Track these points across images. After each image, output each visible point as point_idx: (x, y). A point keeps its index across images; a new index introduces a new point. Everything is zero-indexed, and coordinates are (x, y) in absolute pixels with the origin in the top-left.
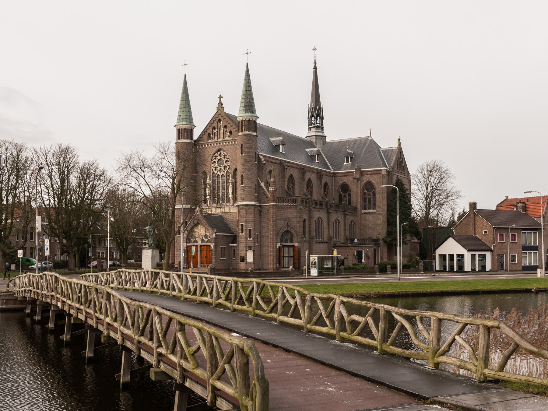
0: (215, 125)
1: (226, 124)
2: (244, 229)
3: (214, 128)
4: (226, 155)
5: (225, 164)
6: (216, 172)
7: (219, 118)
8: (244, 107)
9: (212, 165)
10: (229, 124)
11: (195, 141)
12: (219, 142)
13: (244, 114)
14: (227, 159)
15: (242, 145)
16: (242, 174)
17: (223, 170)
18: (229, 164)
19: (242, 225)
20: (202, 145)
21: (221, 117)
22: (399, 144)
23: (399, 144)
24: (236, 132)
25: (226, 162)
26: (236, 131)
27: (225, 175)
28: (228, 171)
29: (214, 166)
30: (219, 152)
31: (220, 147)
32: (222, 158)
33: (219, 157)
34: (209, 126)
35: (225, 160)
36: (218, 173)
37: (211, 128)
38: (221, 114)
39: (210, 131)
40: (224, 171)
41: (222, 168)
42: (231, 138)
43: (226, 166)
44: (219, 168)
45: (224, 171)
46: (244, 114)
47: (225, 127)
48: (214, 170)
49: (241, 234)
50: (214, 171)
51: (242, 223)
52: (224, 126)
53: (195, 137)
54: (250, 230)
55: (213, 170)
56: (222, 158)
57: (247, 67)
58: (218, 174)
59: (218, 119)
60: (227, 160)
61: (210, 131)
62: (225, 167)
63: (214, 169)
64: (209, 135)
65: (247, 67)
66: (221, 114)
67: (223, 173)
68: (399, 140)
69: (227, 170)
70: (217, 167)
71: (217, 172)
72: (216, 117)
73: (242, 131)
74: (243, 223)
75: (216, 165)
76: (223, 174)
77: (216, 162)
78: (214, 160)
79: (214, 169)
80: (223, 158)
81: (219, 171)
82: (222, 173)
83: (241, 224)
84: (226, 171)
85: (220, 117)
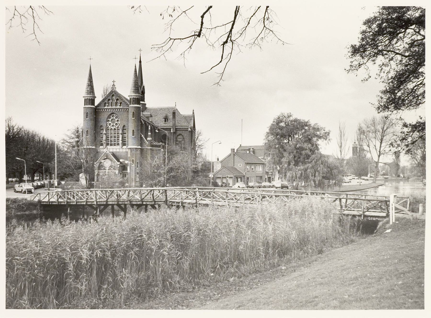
0: (110, 98)
1: (118, 98)
3: (109, 100)
4: (117, 117)
5: (116, 122)
6: (110, 127)
9: (107, 122)
11: (96, 107)
13: (135, 95)
15: (133, 112)
18: (119, 122)
20: (100, 110)
22: (193, 113)
23: (193, 113)
31: (113, 112)
33: (112, 118)
35: (116, 120)
37: (107, 100)
41: (114, 124)
42: (121, 107)
46: (135, 95)
47: (117, 100)
53: (96, 103)
54: (138, 163)
55: (107, 125)
56: (114, 118)
57: (135, 66)
59: (112, 95)
61: (106, 101)
62: (116, 124)
63: (108, 125)
65: (135, 66)
68: (193, 110)
73: (133, 104)
75: (110, 122)
79: (108, 125)
82: (114, 127)
84: (117, 127)
85: (114, 93)
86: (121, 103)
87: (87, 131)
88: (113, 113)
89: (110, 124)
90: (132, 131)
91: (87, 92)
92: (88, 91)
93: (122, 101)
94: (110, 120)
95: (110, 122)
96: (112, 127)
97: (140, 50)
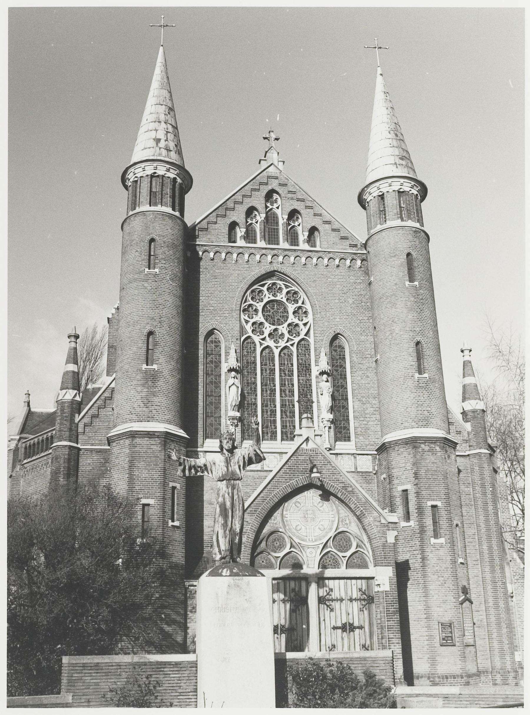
1: (297, 206)
2: (443, 523)
4: (296, 293)
5: (291, 319)
6: (256, 339)
7: (270, 188)
8: (402, 159)
10: (307, 207)
12: (273, 252)
14: (300, 304)
15: (409, 254)
16: (418, 339)
17: (287, 335)
18: (310, 318)
19: (434, 507)
21: (280, 185)
24: (334, 234)
25: (294, 313)
26: (334, 230)
27: (294, 349)
28: (303, 339)
29: (252, 321)
30: (269, 282)
31: (275, 267)
32: (282, 297)
33: (268, 297)
34: (235, 203)
36: (265, 344)
38: (276, 178)
39: (239, 215)
41: (283, 329)
43: (297, 325)
44: (268, 328)
47: (293, 214)
49: (433, 540)
50: (250, 334)
51: (434, 503)
52: (289, 210)
60: (300, 308)
63: (249, 328)
64: (233, 226)
66: (276, 178)
67: (288, 344)
69: (302, 336)
70: (261, 324)
71: (263, 339)
72: (261, 184)
74: (439, 503)
75: (259, 318)
76: (286, 347)
77: (260, 309)
78: (252, 302)
80: (284, 300)
81: (270, 335)
82: (282, 344)
83: (430, 503)
84: (297, 340)
85: (274, 185)
86: (313, 230)
87: (150, 333)
88: (270, 275)
89: (258, 327)
90: (412, 349)
91: (153, 143)
92: (158, 141)
93: (316, 222)
94: (260, 306)
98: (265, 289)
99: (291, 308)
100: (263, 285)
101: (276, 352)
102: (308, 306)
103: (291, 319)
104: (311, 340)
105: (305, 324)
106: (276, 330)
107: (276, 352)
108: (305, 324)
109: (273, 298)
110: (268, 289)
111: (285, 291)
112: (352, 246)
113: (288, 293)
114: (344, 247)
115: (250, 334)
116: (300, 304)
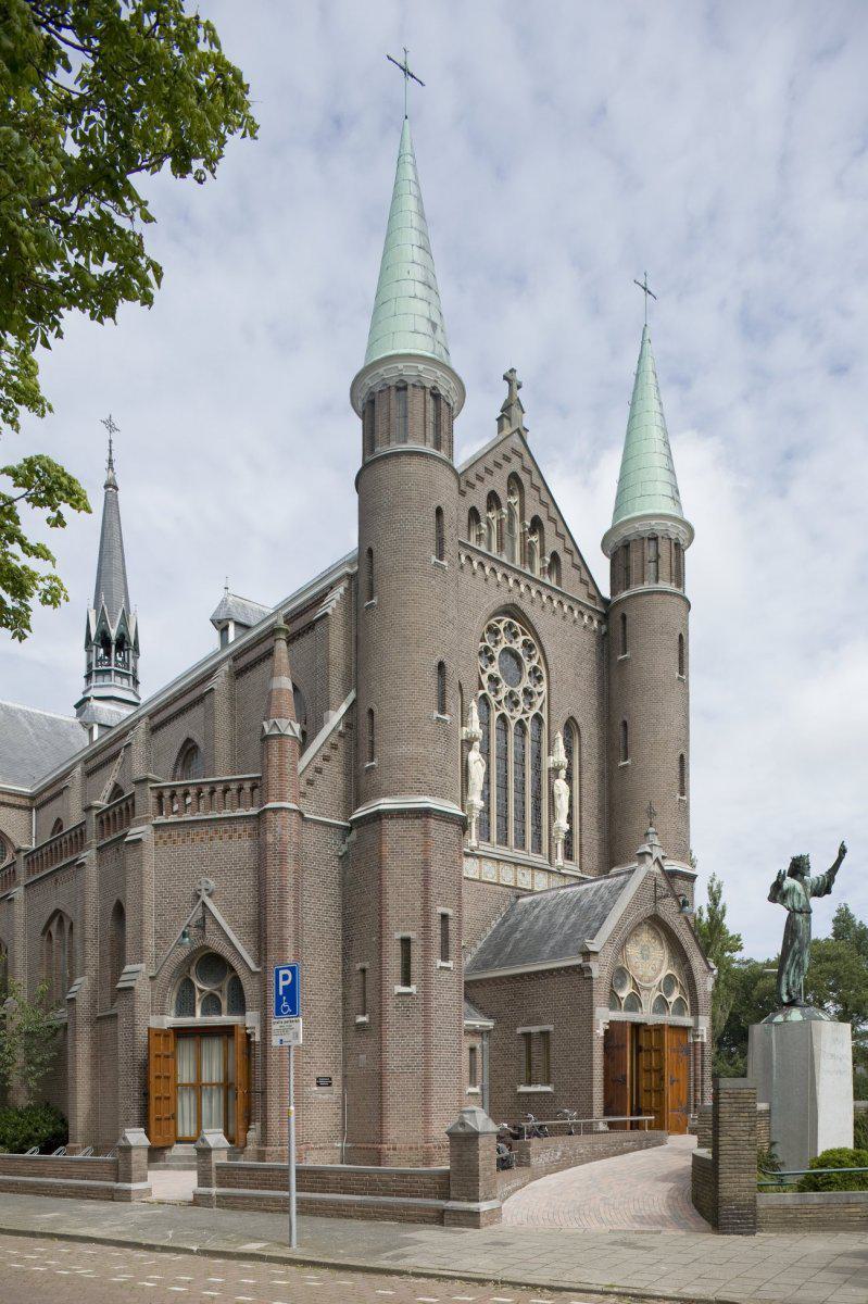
6: (493, 701)
18: (543, 687)
31: (517, 600)
32: (517, 645)
40: (524, 712)
41: (519, 690)
44: (504, 689)
45: (524, 712)
48: (486, 685)
50: (486, 691)
58: (503, 717)
67: (524, 717)
69: (536, 710)
71: (499, 703)
76: (520, 722)
78: (488, 644)
79: (485, 678)
80: (520, 651)
82: (518, 716)
84: (531, 714)
95: (494, 669)
96: (508, 713)
97: (110, 425)
98: (501, 627)
99: (528, 666)
100: (499, 622)
101: (513, 723)
102: (542, 668)
103: (526, 682)
104: (544, 716)
105: (540, 694)
106: (511, 694)
107: (513, 723)
108: (540, 694)
109: (508, 645)
110: (505, 629)
111: (521, 638)
112: (591, 597)
113: (525, 643)
114: (580, 594)
115: (486, 691)
116: (534, 663)
